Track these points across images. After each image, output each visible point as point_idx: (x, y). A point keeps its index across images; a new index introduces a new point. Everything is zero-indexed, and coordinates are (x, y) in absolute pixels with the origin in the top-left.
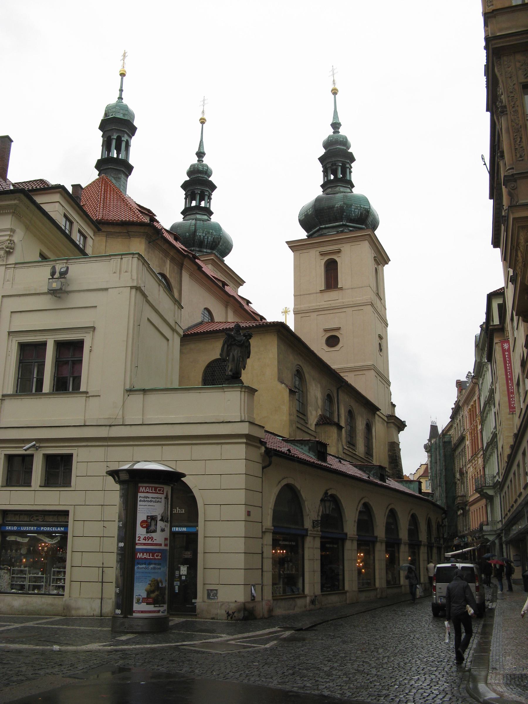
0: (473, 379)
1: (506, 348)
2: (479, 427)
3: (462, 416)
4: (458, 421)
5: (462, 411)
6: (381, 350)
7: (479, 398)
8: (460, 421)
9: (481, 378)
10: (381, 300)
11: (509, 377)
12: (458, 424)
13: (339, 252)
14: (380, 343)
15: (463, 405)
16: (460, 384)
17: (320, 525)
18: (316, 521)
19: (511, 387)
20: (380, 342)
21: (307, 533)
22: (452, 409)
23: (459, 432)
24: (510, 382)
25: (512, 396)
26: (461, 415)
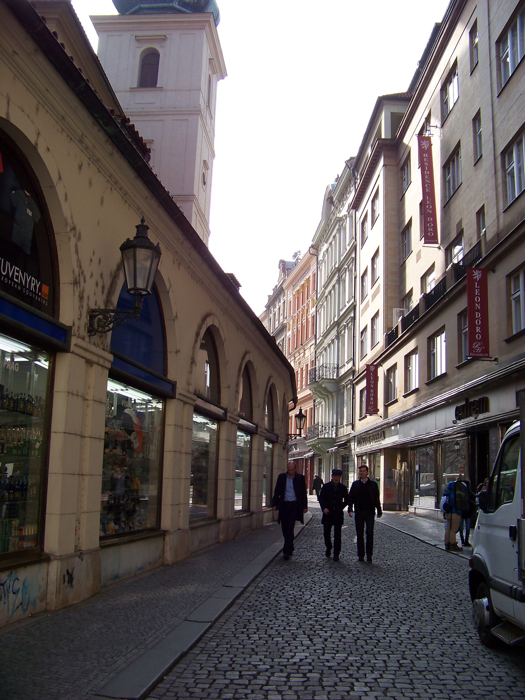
0: (311, 249)
1: (425, 148)
2: (312, 311)
3: (284, 302)
4: (276, 310)
5: (284, 296)
6: (205, 183)
7: (315, 276)
8: (279, 308)
9: (326, 243)
10: (212, 119)
11: (427, 191)
12: (275, 314)
13: (164, 39)
15: (288, 287)
17: (111, 326)
19: (429, 207)
20: (204, 171)
21: (68, 342)
22: (269, 296)
23: (277, 323)
24: (428, 199)
25: (430, 219)
26: (282, 301)
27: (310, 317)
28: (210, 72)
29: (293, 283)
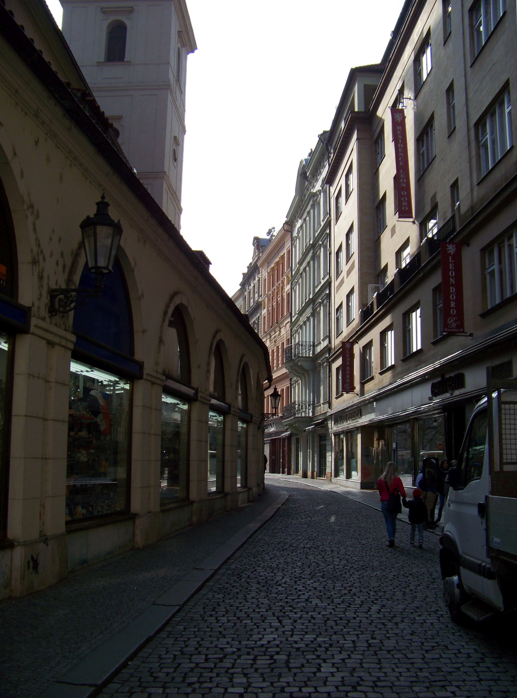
1: (398, 120)
2: (287, 288)
3: (259, 280)
4: (251, 287)
5: (259, 273)
6: (175, 160)
7: (290, 252)
8: (254, 286)
9: (300, 218)
10: (182, 93)
11: (401, 164)
12: (250, 292)
13: (131, 10)
14: (174, 149)
15: (262, 265)
16: (258, 243)
17: (73, 305)
18: (62, 291)
19: (403, 180)
20: (174, 147)
21: (27, 323)
22: (243, 274)
23: (252, 301)
24: (401, 172)
25: (404, 193)
26: (257, 279)
27: (285, 294)
28: (179, 45)
29: (268, 261)
